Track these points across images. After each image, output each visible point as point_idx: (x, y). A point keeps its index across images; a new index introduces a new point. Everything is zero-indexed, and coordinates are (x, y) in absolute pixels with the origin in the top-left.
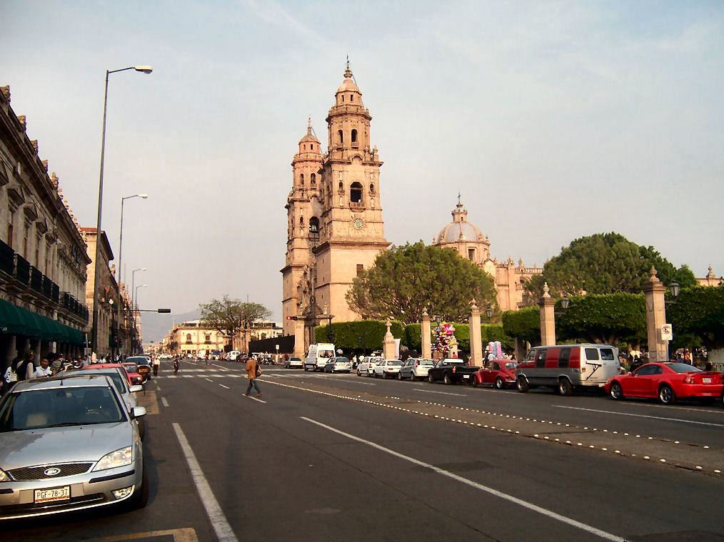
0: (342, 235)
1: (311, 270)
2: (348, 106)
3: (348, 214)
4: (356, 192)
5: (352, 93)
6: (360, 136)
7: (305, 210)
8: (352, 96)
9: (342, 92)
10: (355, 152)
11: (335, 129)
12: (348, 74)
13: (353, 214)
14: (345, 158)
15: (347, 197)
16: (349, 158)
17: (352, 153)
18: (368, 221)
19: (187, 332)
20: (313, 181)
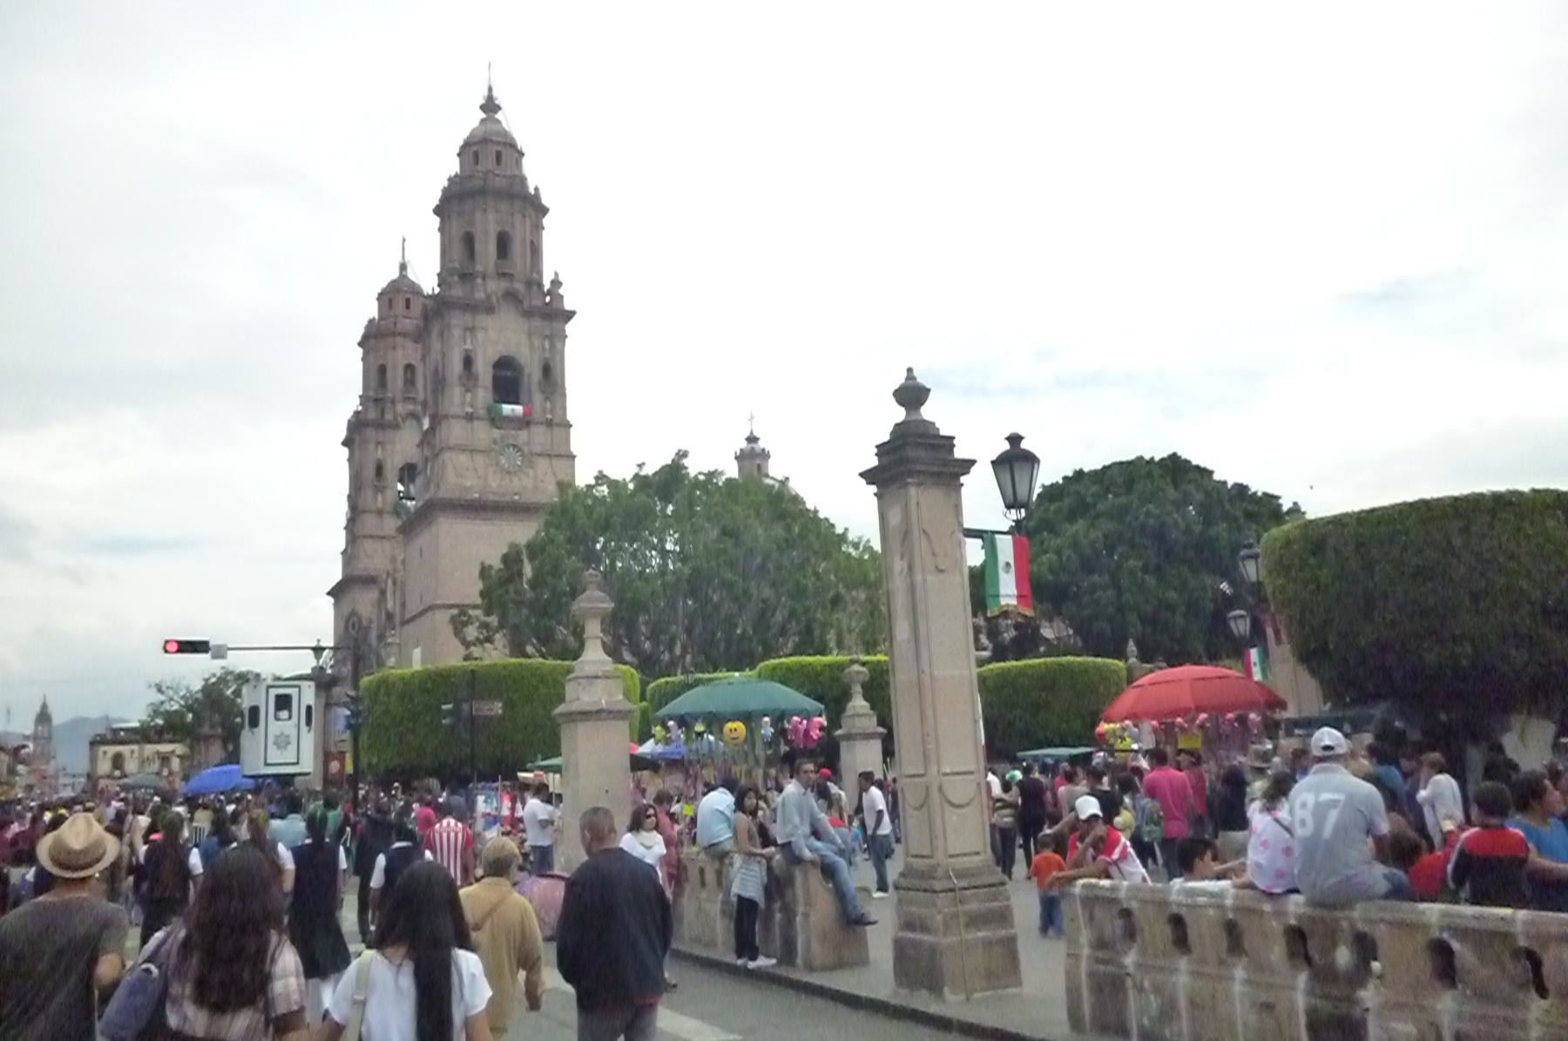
0: (469, 484)
1: (394, 583)
3: (483, 433)
4: (507, 381)
5: (499, 148)
6: (518, 250)
7: (389, 447)
10: (504, 285)
11: (457, 230)
12: (490, 106)
13: (497, 433)
14: (480, 295)
15: (484, 394)
17: (495, 286)
18: (538, 449)
19: (112, 750)
20: (410, 381)
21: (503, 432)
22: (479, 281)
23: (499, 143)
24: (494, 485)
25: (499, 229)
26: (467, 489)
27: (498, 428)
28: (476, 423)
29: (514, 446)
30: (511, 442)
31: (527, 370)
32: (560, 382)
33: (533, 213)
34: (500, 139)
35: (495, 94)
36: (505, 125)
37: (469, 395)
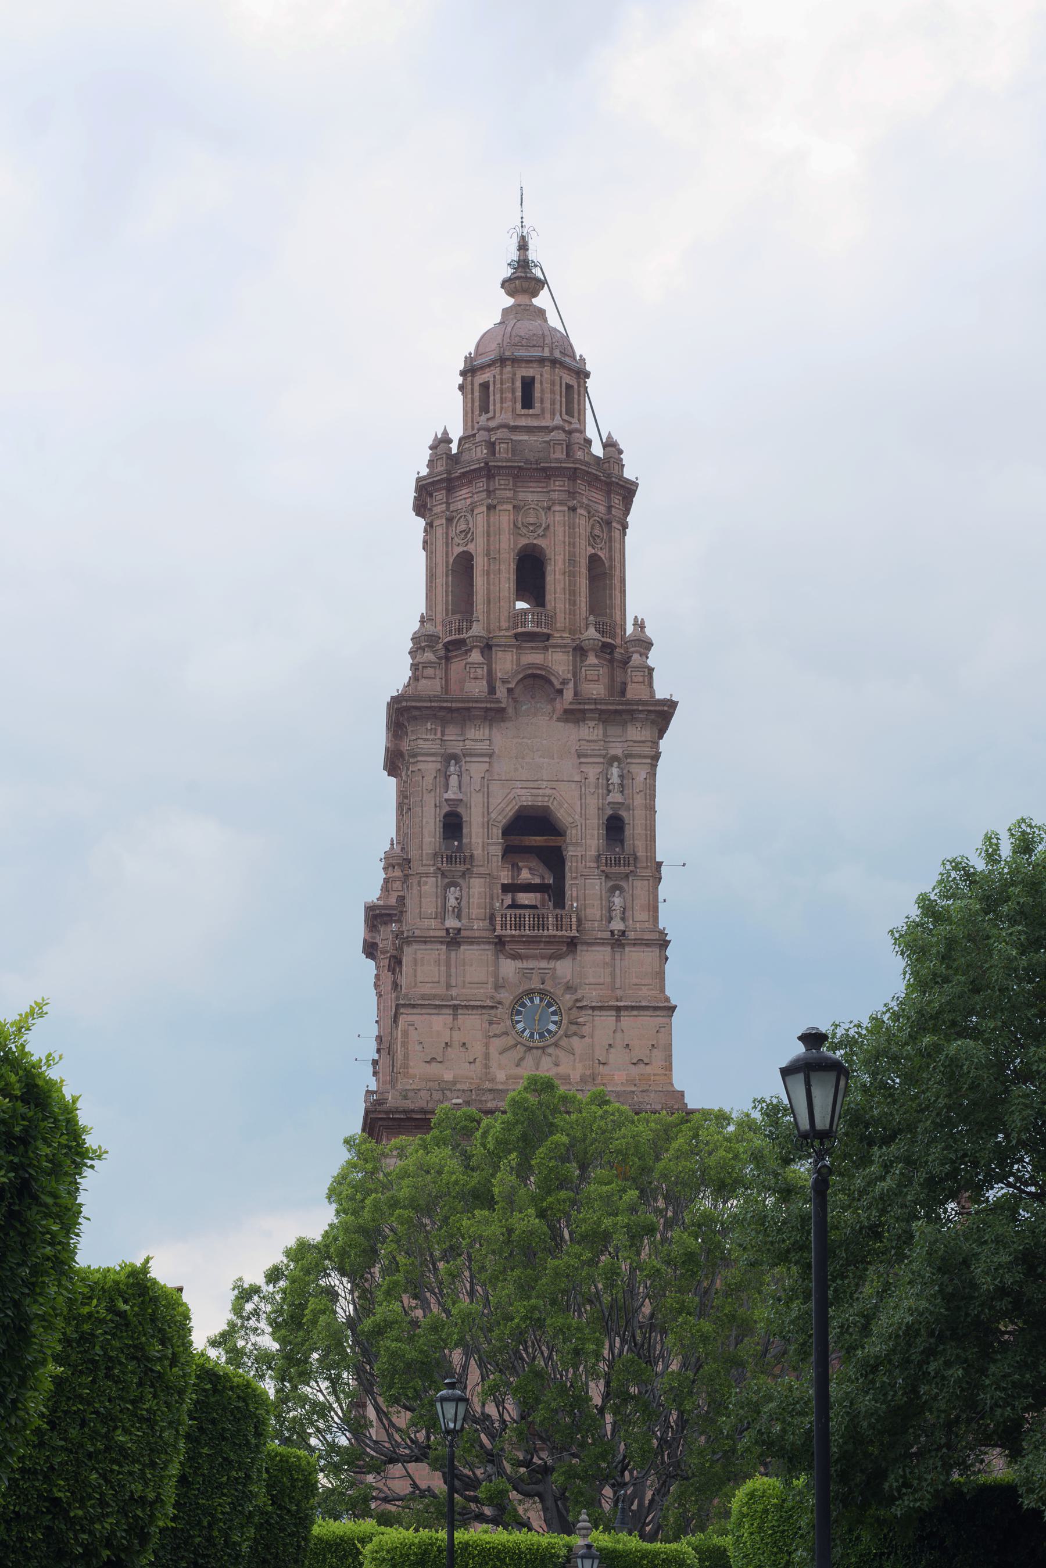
0: (448, 1076)
2: (500, 434)
5: (529, 372)
8: (528, 385)
9: (482, 368)
10: (533, 658)
13: (509, 968)
14: (477, 688)
16: (492, 690)
18: (592, 996)
21: (519, 964)
22: (476, 656)
23: (529, 361)
24: (501, 1076)
25: (524, 541)
26: (445, 1088)
27: (516, 957)
28: (467, 952)
29: (543, 993)
30: (535, 984)
31: (572, 834)
32: (641, 853)
33: (598, 496)
34: (536, 353)
35: (532, 256)
36: (553, 321)
37: (453, 893)
